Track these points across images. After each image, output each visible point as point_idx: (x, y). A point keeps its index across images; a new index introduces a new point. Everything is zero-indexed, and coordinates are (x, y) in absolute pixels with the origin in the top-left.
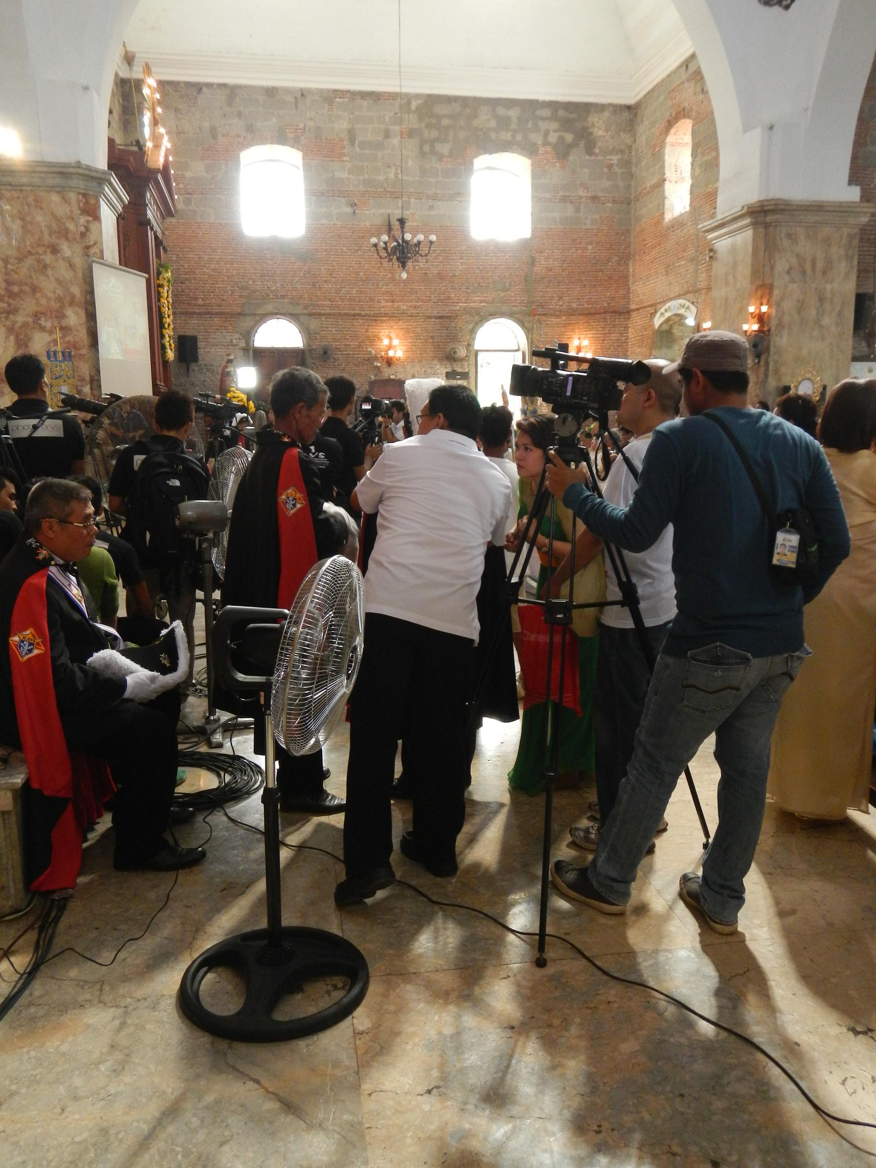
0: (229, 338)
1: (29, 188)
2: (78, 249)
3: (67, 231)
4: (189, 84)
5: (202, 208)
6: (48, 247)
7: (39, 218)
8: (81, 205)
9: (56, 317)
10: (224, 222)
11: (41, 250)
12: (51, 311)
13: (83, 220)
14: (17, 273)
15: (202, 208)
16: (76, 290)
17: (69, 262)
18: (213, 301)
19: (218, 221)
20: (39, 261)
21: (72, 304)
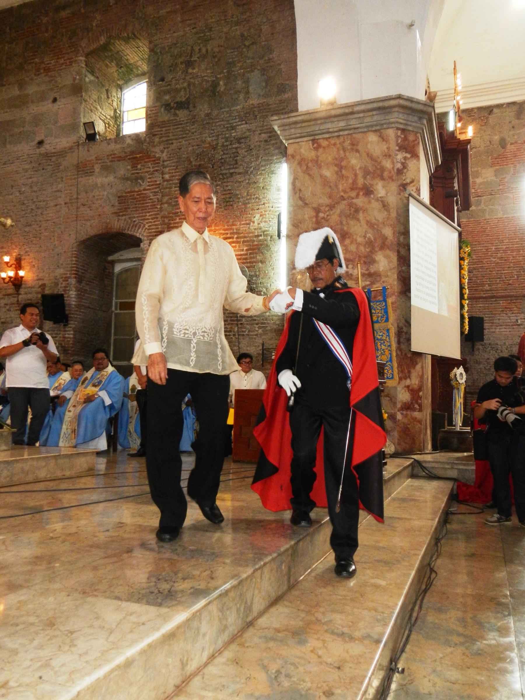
0: (513, 319)
1: (346, 132)
2: (394, 187)
3: (383, 169)
4: (480, 109)
5: (491, 207)
6: (362, 189)
7: (354, 161)
8: (399, 141)
9: (365, 263)
10: (511, 216)
11: (353, 194)
12: (359, 257)
13: (400, 156)
14: (327, 221)
15: (491, 207)
16: (388, 232)
17: (382, 201)
18: (500, 285)
19: (505, 216)
20: (351, 205)
21: (383, 247)
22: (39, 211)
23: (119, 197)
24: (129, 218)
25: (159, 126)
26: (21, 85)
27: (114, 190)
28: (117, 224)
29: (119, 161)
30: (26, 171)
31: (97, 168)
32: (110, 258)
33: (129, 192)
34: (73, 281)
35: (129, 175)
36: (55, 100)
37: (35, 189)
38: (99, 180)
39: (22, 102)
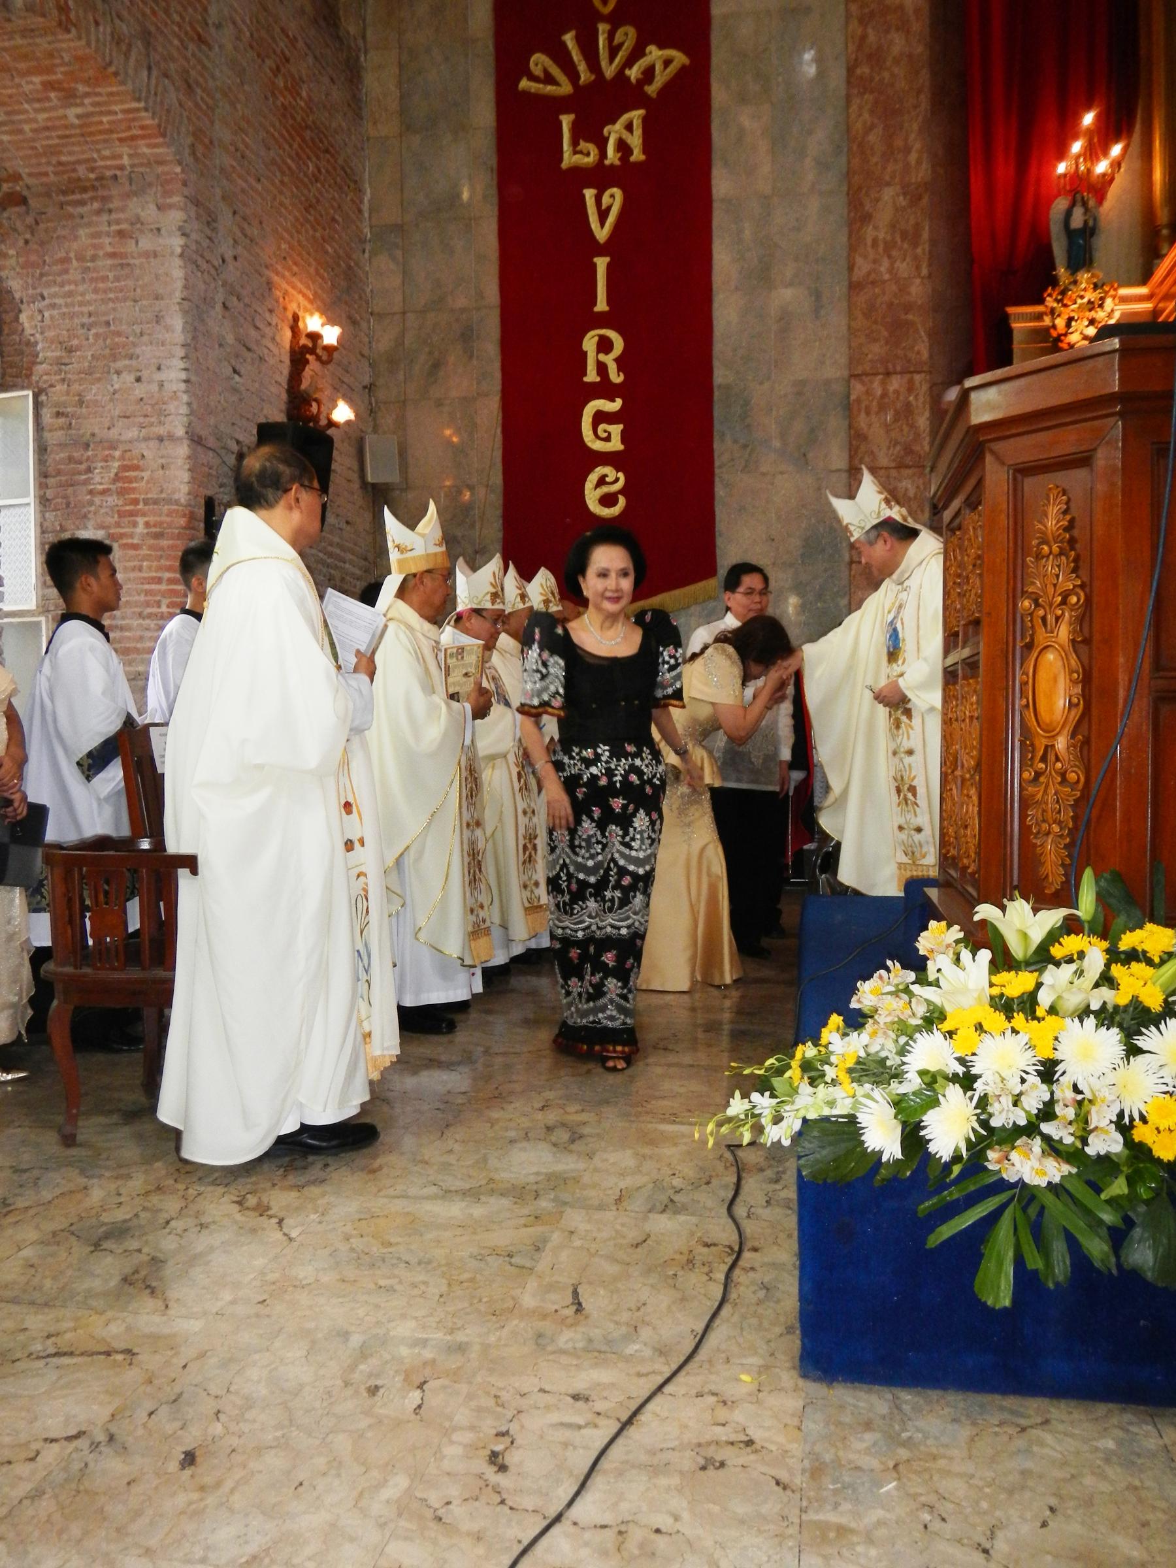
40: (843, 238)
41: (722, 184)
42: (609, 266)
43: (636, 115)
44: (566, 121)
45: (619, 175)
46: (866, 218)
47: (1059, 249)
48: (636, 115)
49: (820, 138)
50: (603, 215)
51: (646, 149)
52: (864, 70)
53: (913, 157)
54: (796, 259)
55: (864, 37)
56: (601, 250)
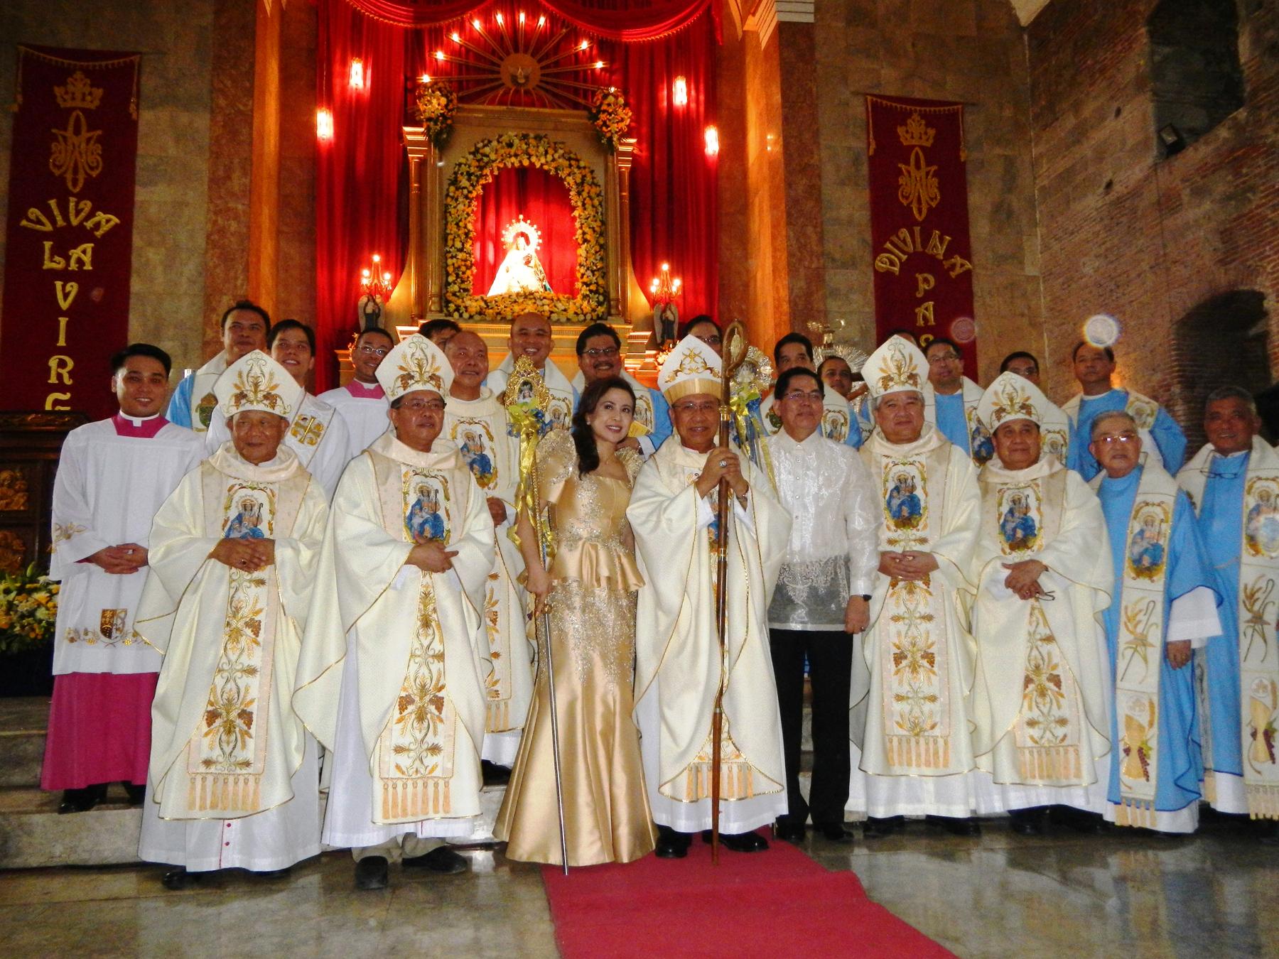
22: (1121, 290)
23: (1222, 233)
24: (1242, 263)
25: (1265, 89)
26: (1077, 107)
27: (1213, 224)
28: (1223, 278)
29: (1213, 172)
30: (1097, 234)
31: (1186, 195)
32: (1253, 332)
33: (1235, 220)
34: (1176, 389)
35: (1232, 190)
36: (1118, 112)
37: (1112, 258)
38: (1192, 213)
39: (1080, 133)
40: (200, 319)
41: (136, 285)
42: (68, 324)
43: (89, 246)
44: (48, 245)
45: (78, 275)
46: (214, 310)
47: (363, 323)
48: (89, 246)
49: (190, 268)
50: (66, 296)
51: (93, 263)
52: (216, 237)
53: (239, 282)
54: (176, 327)
55: (215, 222)
56: (64, 314)
